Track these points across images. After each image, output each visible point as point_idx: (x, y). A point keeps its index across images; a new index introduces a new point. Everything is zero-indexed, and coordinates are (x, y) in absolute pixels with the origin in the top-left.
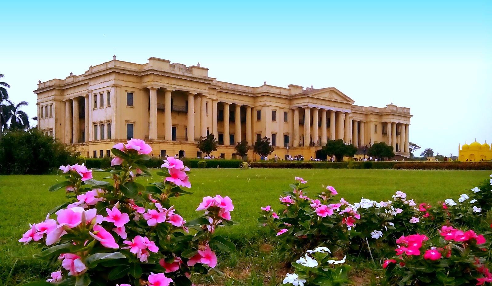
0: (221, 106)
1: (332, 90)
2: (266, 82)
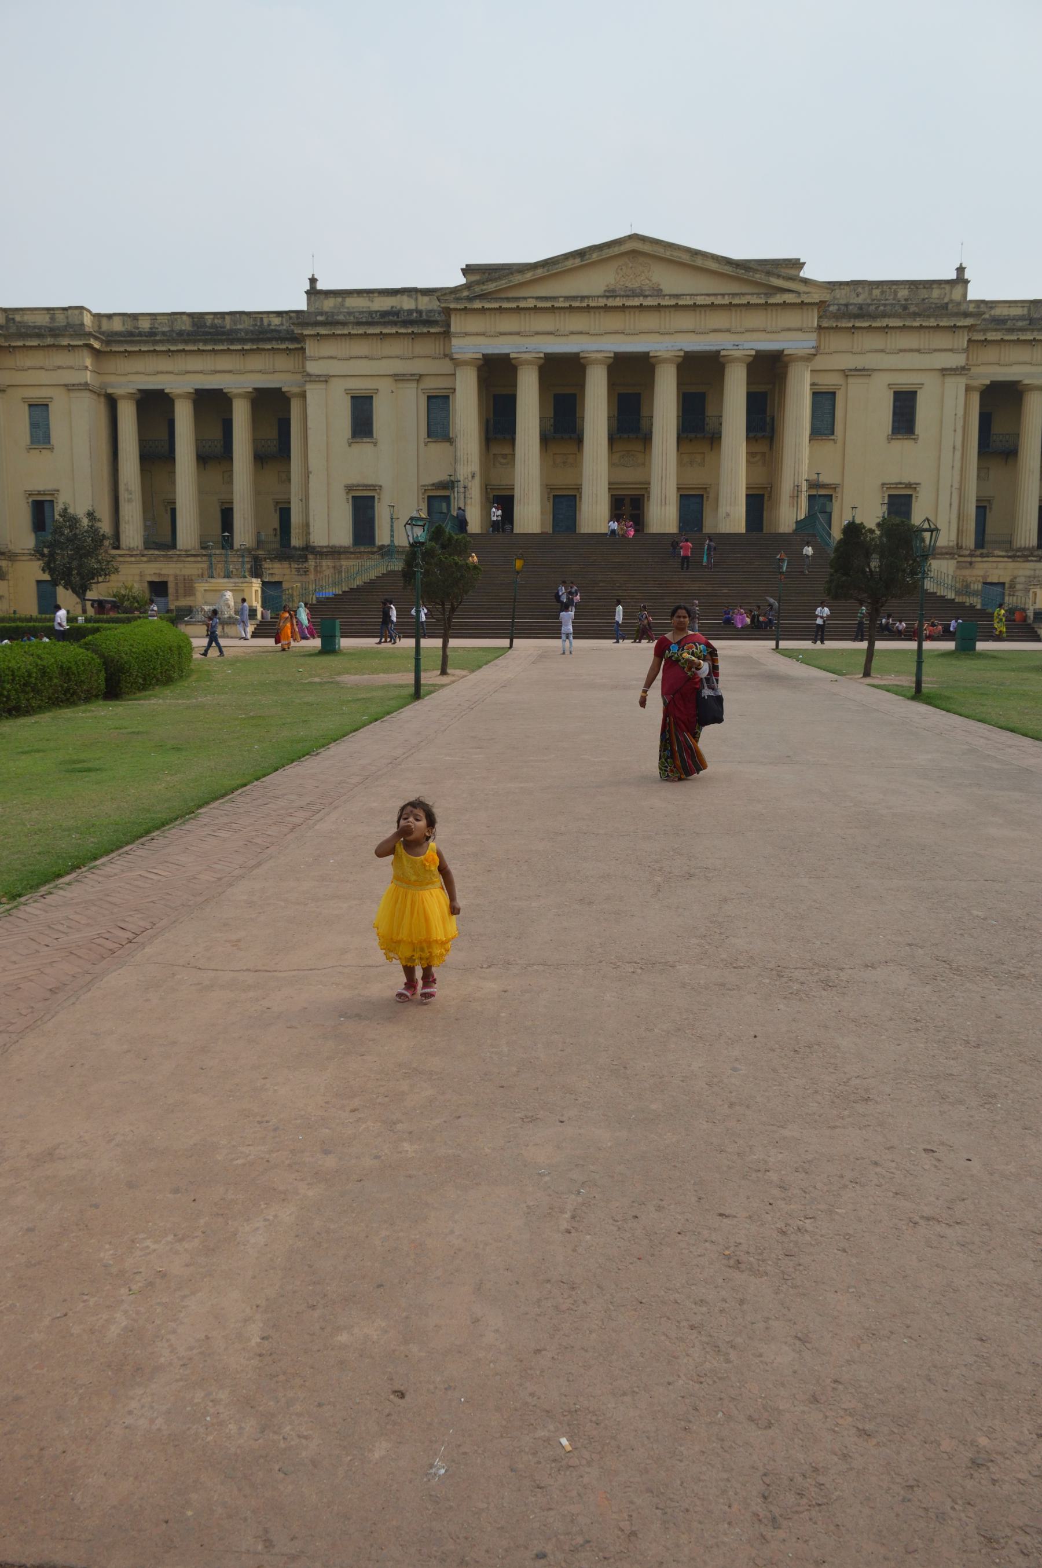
1: (634, 253)
2: (316, 280)
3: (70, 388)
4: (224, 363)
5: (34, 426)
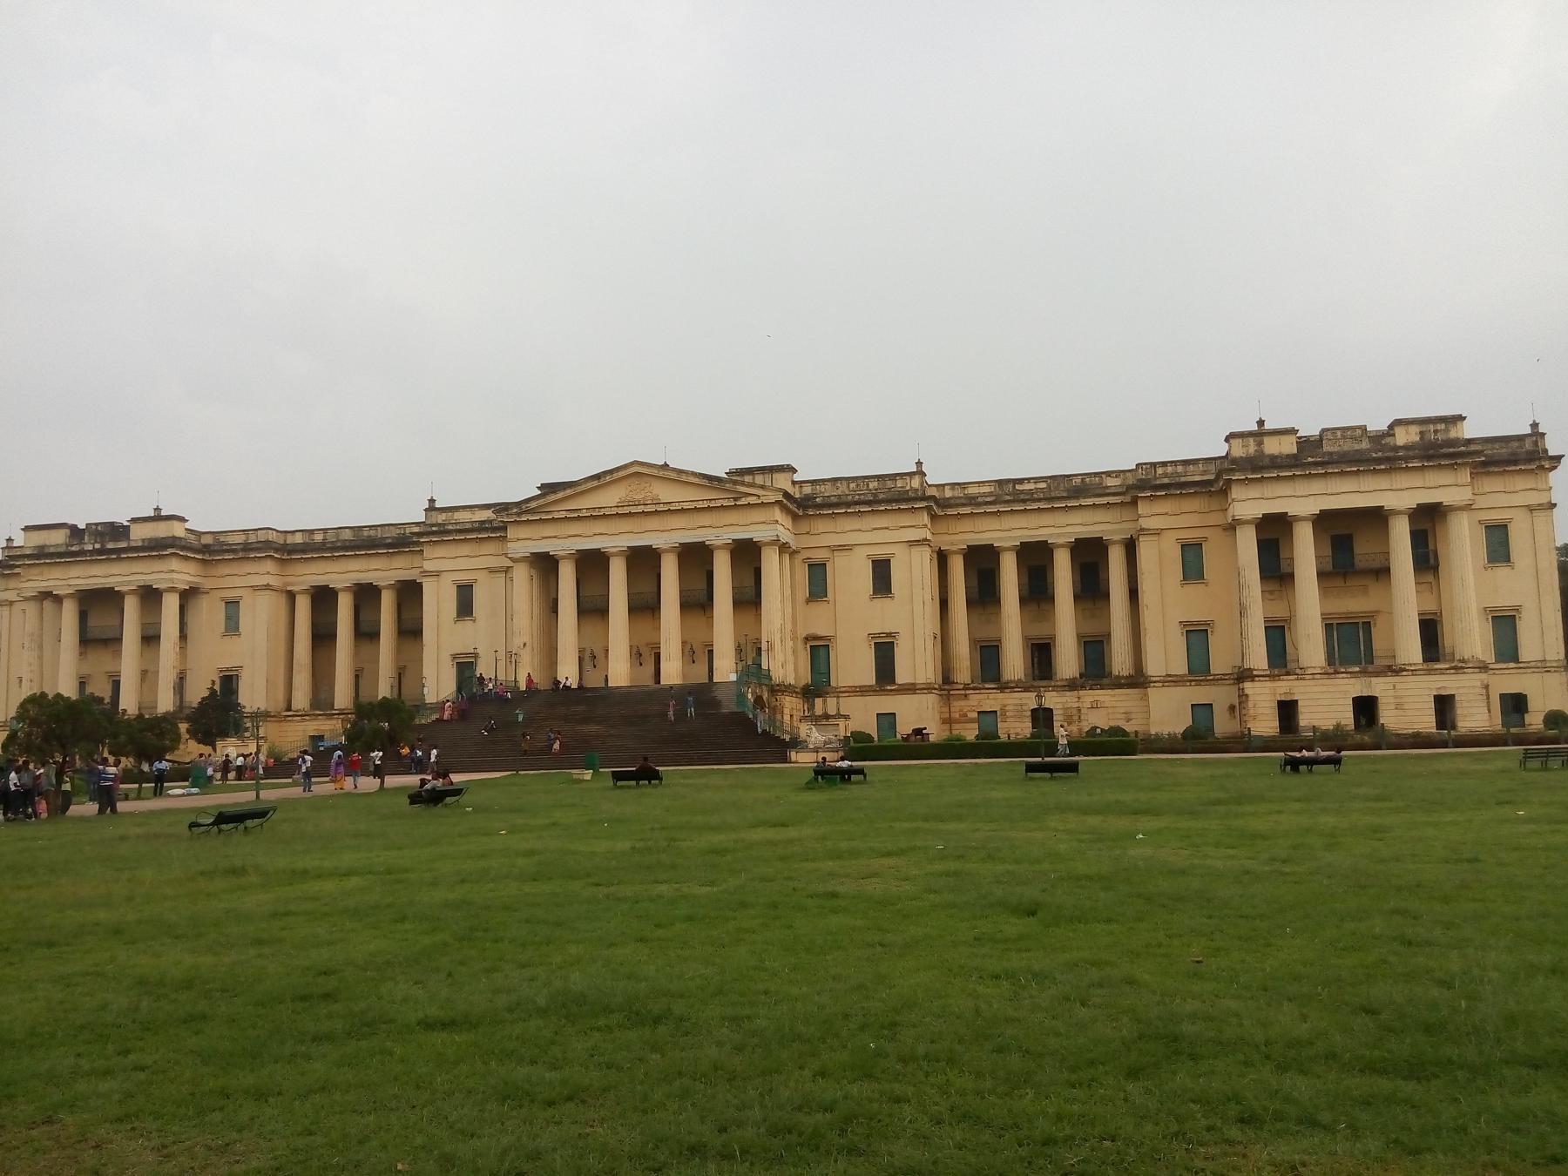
0: (323, 598)
3: (255, 588)
4: (375, 563)
5: (228, 618)
